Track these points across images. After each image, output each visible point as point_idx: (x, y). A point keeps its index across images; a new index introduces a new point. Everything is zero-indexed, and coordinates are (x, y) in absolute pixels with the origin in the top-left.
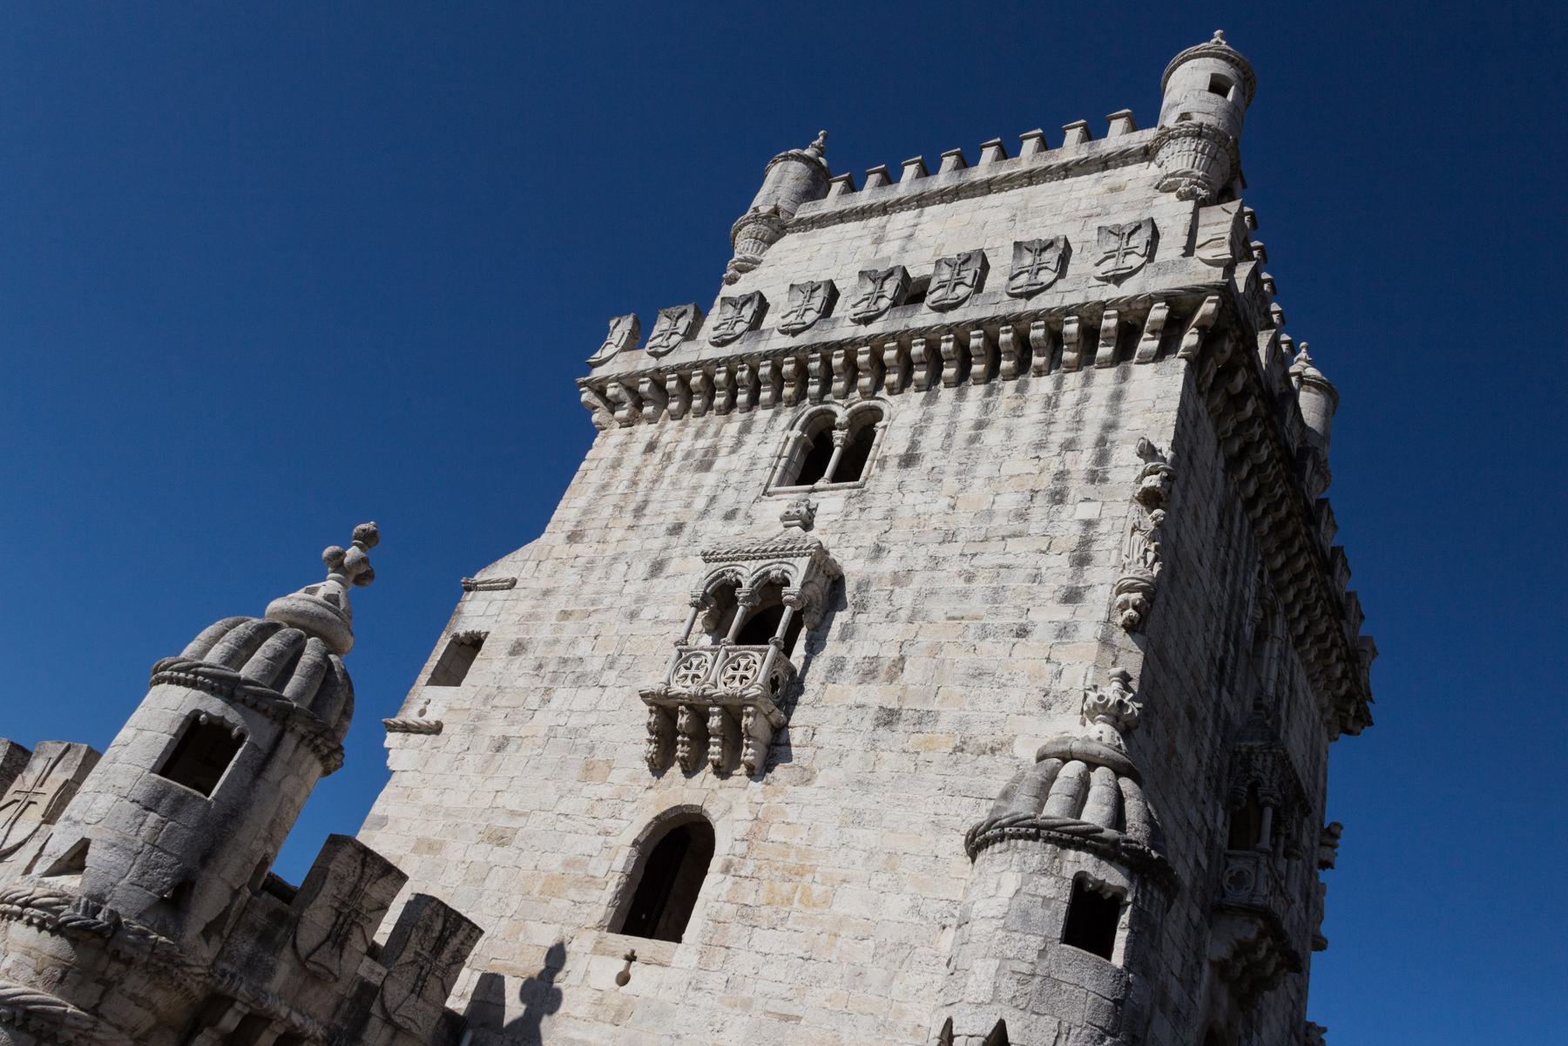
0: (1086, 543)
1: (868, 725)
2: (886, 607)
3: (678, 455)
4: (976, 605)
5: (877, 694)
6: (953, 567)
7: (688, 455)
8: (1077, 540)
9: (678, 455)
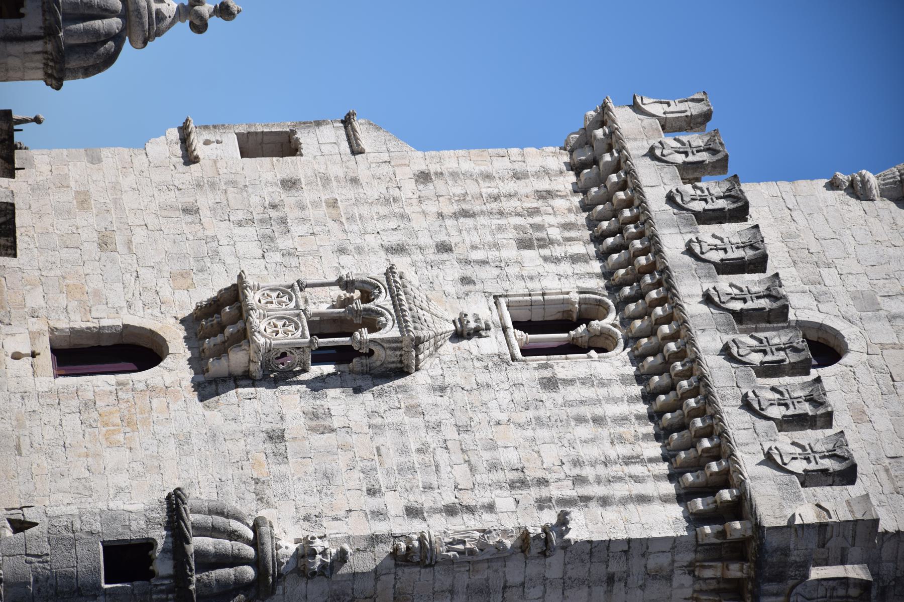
0: (470, 510)
1: (267, 427)
2: (384, 407)
3: (537, 220)
4: (392, 460)
5: (295, 425)
6: (432, 439)
7: (538, 227)
8: (472, 503)
9: (537, 220)
